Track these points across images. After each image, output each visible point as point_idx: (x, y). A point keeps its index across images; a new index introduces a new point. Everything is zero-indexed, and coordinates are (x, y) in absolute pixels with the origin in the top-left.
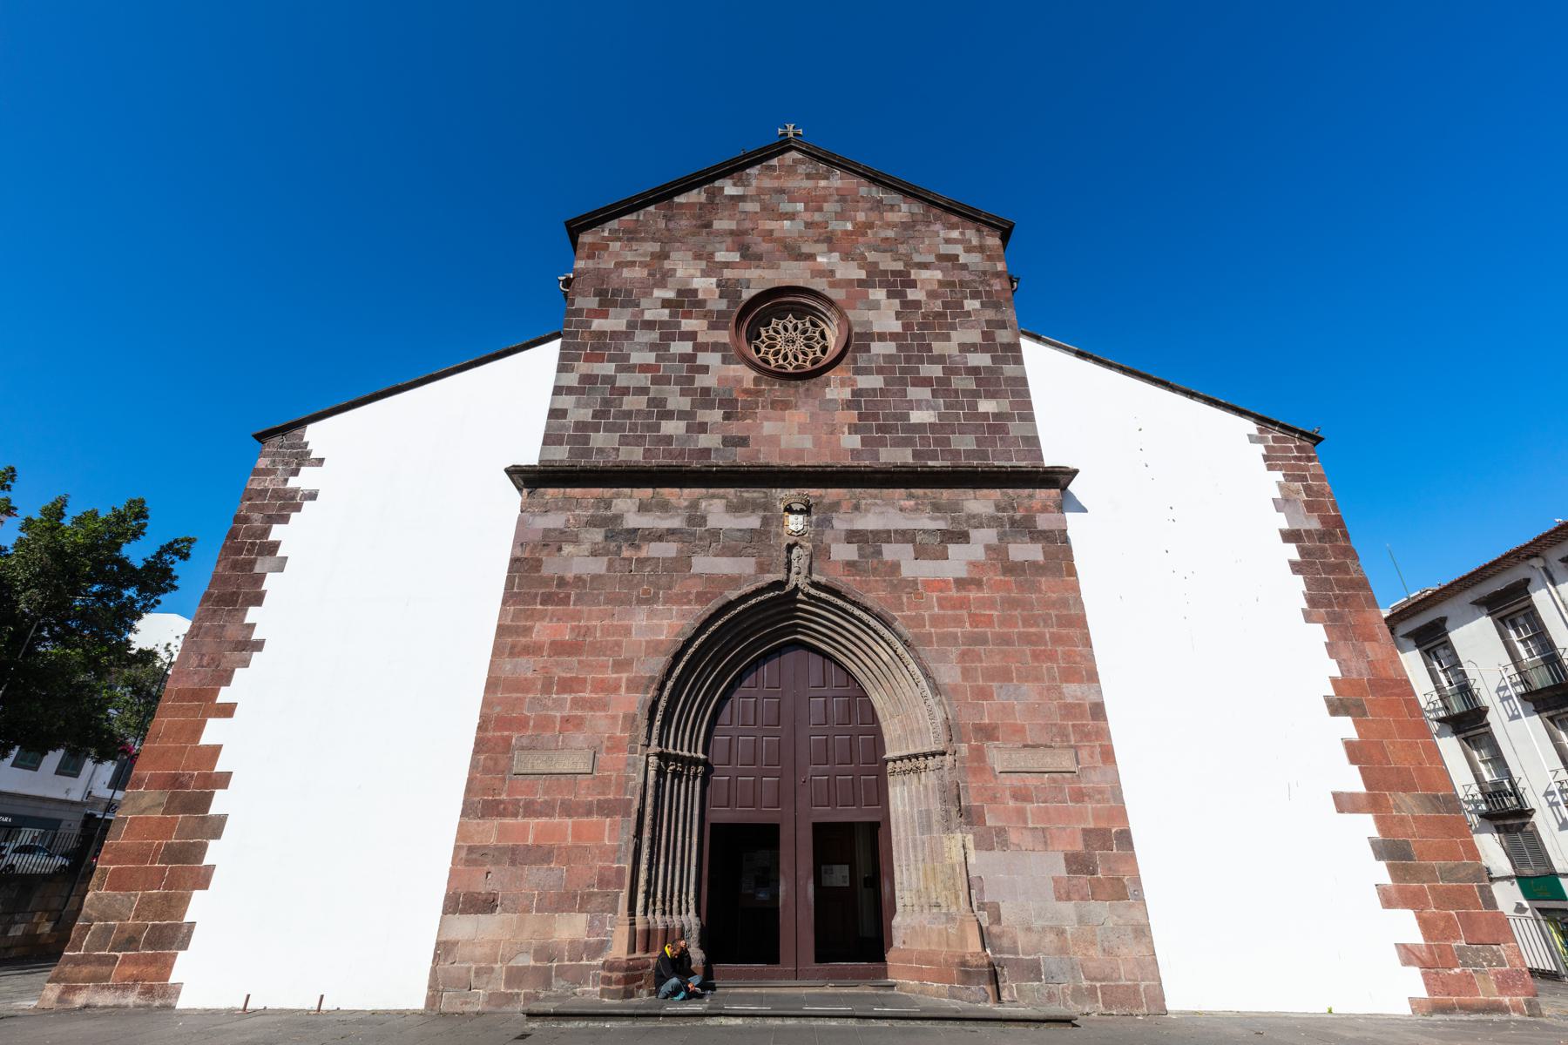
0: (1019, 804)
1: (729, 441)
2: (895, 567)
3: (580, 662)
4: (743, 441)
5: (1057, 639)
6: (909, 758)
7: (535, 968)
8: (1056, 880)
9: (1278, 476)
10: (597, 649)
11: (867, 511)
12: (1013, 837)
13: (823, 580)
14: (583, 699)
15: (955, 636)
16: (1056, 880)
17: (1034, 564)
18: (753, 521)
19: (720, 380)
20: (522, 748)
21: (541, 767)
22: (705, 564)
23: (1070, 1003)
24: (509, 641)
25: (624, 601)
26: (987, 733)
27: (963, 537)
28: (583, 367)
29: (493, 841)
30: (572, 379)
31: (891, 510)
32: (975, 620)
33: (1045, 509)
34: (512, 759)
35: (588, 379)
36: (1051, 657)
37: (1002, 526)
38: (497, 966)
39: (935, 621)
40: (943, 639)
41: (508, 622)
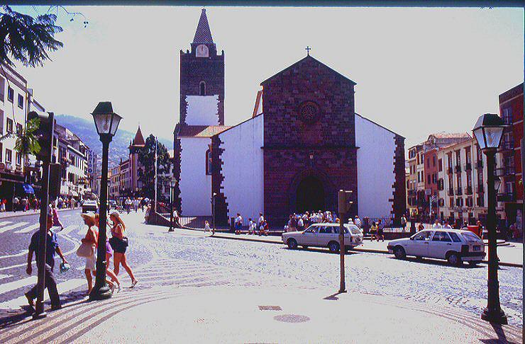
9: (396, 146)
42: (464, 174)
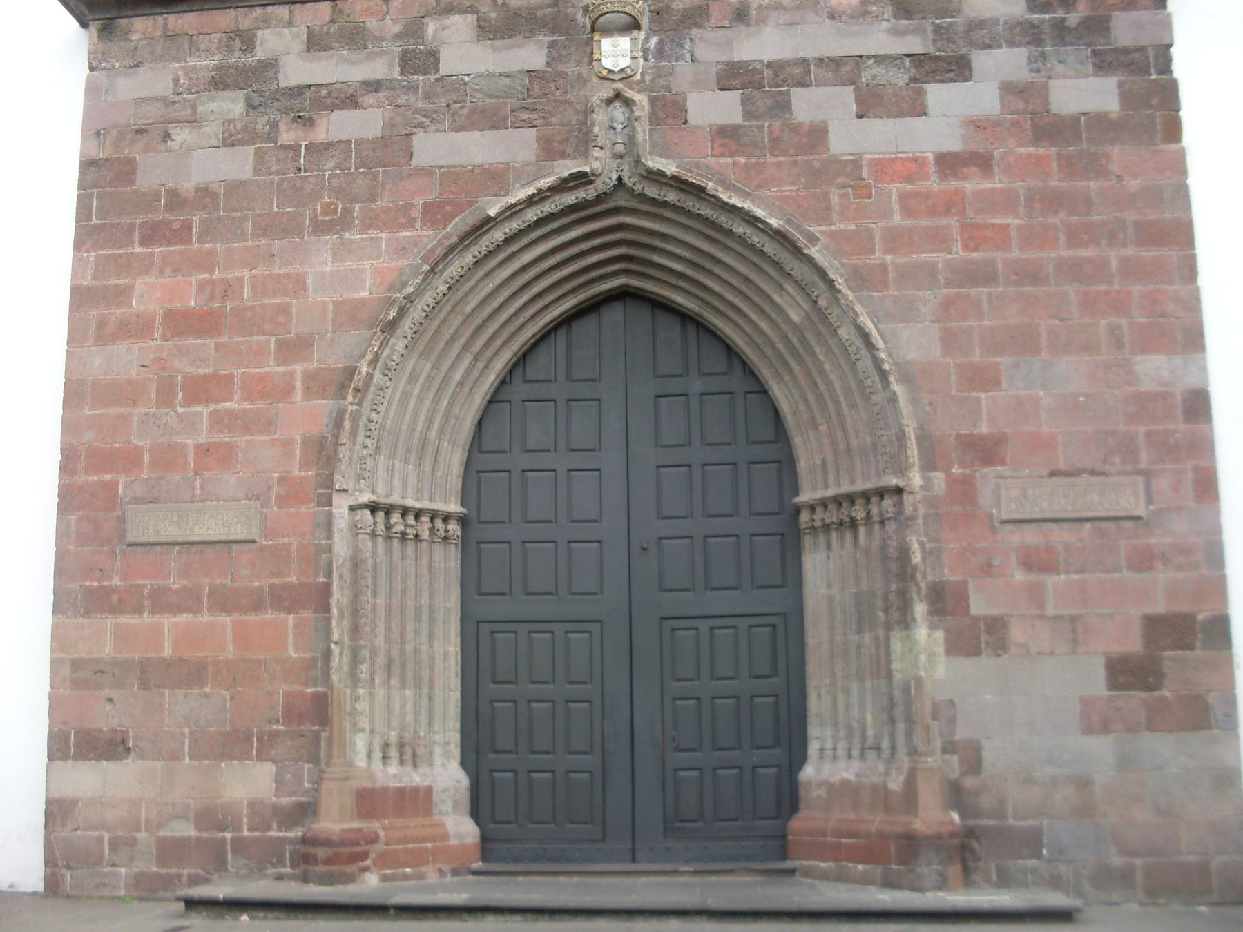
0: (1033, 577)
2: (818, 135)
3: (217, 346)
5: (1132, 270)
6: (838, 501)
7: (199, 839)
8: (1085, 702)
11: (762, 21)
12: (1017, 633)
13: (670, 168)
14: (231, 414)
15: (931, 269)
16: (1085, 702)
17: (1099, 120)
20: (136, 501)
21: (170, 531)
22: (438, 148)
23: (1087, 888)
25: (289, 228)
26: (986, 451)
27: (956, 68)
29: (108, 651)
31: (811, 16)
32: (974, 236)
34: (122, 520)
37: (1038, 41)
38: (142, 835)
39: (894, 239)
40: (907, 275)
41: (89, 281)
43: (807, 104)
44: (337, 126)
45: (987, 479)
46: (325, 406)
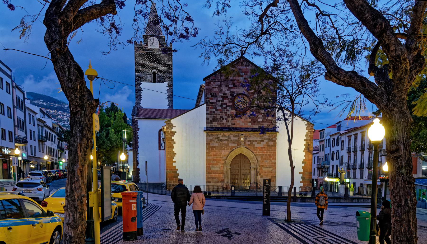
1: (232, 124)
2: (254, 145)
4: (234, 124)
5: (272, 155)
9: (307, 131)
10: (218, 155)
18: (237, 139)
19: (231, 113)
22: (230, 145)
24: (208, 154)
26: (263, 166)
27: (263, 141)
28: (210, 110)
30: (209, 112)
32: (263, 152)
33: (274, 137)
35: (211, 112)
36: (271, 157)
39: (259, 152)
42: (359, 153)
43: (254, 143)
44: (224, 142)
45: (263, 167)
46: (224, 161)
